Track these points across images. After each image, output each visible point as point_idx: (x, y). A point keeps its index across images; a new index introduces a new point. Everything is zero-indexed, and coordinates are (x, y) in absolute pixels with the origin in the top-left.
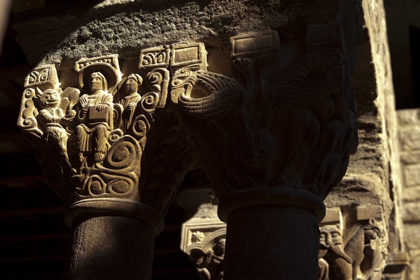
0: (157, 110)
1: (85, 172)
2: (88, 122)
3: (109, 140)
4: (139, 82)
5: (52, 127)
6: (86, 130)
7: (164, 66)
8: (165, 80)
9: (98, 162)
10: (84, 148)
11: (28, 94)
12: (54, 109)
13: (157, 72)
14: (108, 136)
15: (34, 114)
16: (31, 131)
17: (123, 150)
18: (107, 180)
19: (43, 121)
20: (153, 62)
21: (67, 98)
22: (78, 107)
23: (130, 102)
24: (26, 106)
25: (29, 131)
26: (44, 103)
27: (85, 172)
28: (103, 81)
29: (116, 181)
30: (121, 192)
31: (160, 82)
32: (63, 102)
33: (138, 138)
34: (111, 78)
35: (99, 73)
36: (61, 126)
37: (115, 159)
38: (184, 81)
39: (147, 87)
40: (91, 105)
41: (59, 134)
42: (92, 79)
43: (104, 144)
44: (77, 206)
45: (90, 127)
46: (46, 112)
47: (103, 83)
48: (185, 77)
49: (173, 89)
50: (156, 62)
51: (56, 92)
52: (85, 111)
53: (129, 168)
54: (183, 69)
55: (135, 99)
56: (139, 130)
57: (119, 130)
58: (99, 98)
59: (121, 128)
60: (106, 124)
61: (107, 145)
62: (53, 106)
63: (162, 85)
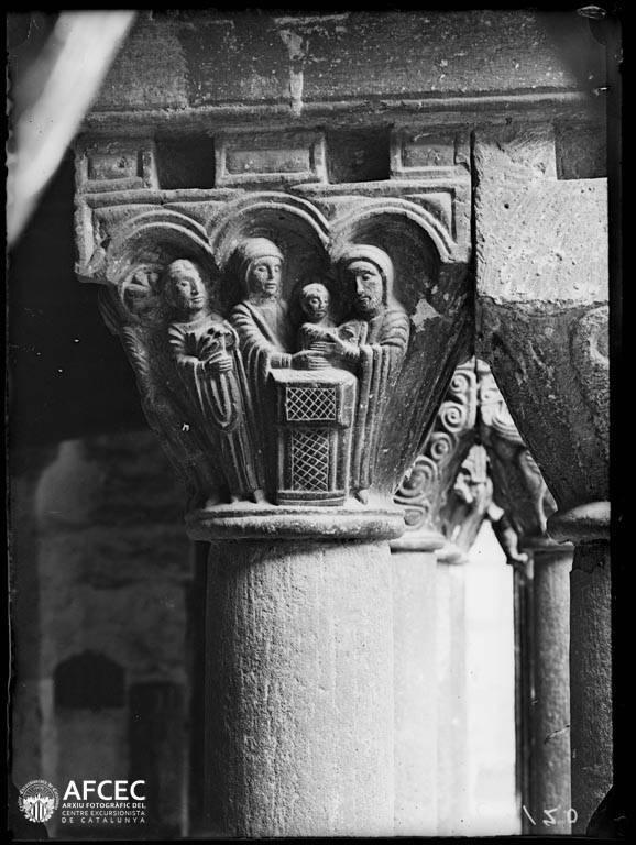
7: (469, 369)
33: (436, 461)
56: (438, 452)
63: (468, 394)
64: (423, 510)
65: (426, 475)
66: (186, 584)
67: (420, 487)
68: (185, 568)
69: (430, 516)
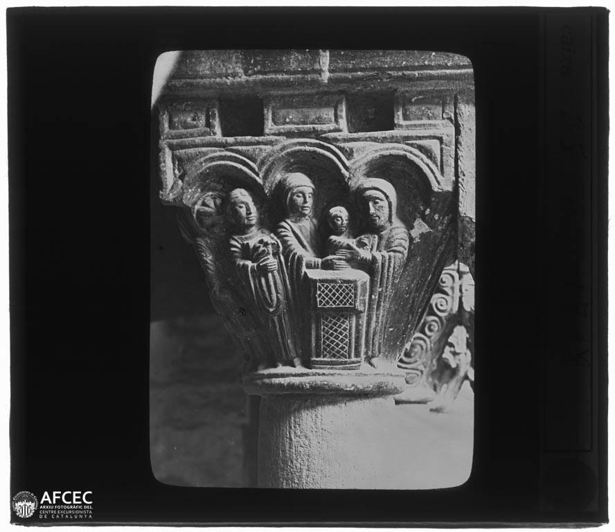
0: (450, 314)
7: (453, 270)
33: (429, 337)
56: (430, 330)
63: (452, 288)
64: (419, 373)
67: (417, 356)
69: (424, 377)
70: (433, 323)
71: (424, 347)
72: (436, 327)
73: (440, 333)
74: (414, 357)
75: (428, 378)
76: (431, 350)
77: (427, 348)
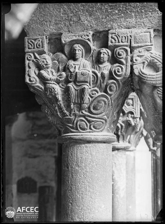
1: (75, 115)
2: (75, 82)
3: (90, 95)
4: (109, 55)
5: (50, 85)
6: (74, 88)
7: (126, 46)
8: (128, 56)
9: (84, 109)
10: (74, 100)
11: (29, 58)
12: (49, 70)
13: (121, 49)
14: (89, 93)
15: (35, 73)
16: (35, 86)
17: (101, 103)
18: (89, 121)
19: (43, 80)
20: (119, 42)
21: (56, 62)
22: (66, 69)
23: (103, 70)
24: (29, 68)
25: (34, 86)
26: (42, 65)
27: (75, 115)
28: (82, 51)
29: (96, 123)
30: (99, 129)
31: (124, 58)
32: (54, 64)
33: (110, 95)
34: (88, 50)
35: (79, 45)
36: (56, 84)
37: (95, 108)
38: (142, 58)
39: (115, 59)
40: (77, 70)
41: (56, 90)
42: (76, 50)
43: (87, 98)
44: (70, 137)
45: (77, 86)
46: (42, 72)
47: (82, 53)
48: (142, 56)
49: (135, 64)
50: (120, 41)
51: (48, 58)
52: (73, 75)
53: (104, 114)
54: (140, 49)
55: (106, 68)
56: (111, 90)
57: (96, 88)
58: (81, 65)
59: (98, 87)
60: (88, 84)
61: (89, 98)
62: (48, 68)
63: (126, 59)
64: (104, 121)
65: (105, 102)
66: (55, 157)
67: (102, 109)
68: (55, 152)
69: (108, 125)
70: (113, 85)
71: (107, 102)
72: (114, 87)
73: (118, 93)
74: (99, 109)
75: (110, 126)
76: (112, 105)
77: (109, 104)
